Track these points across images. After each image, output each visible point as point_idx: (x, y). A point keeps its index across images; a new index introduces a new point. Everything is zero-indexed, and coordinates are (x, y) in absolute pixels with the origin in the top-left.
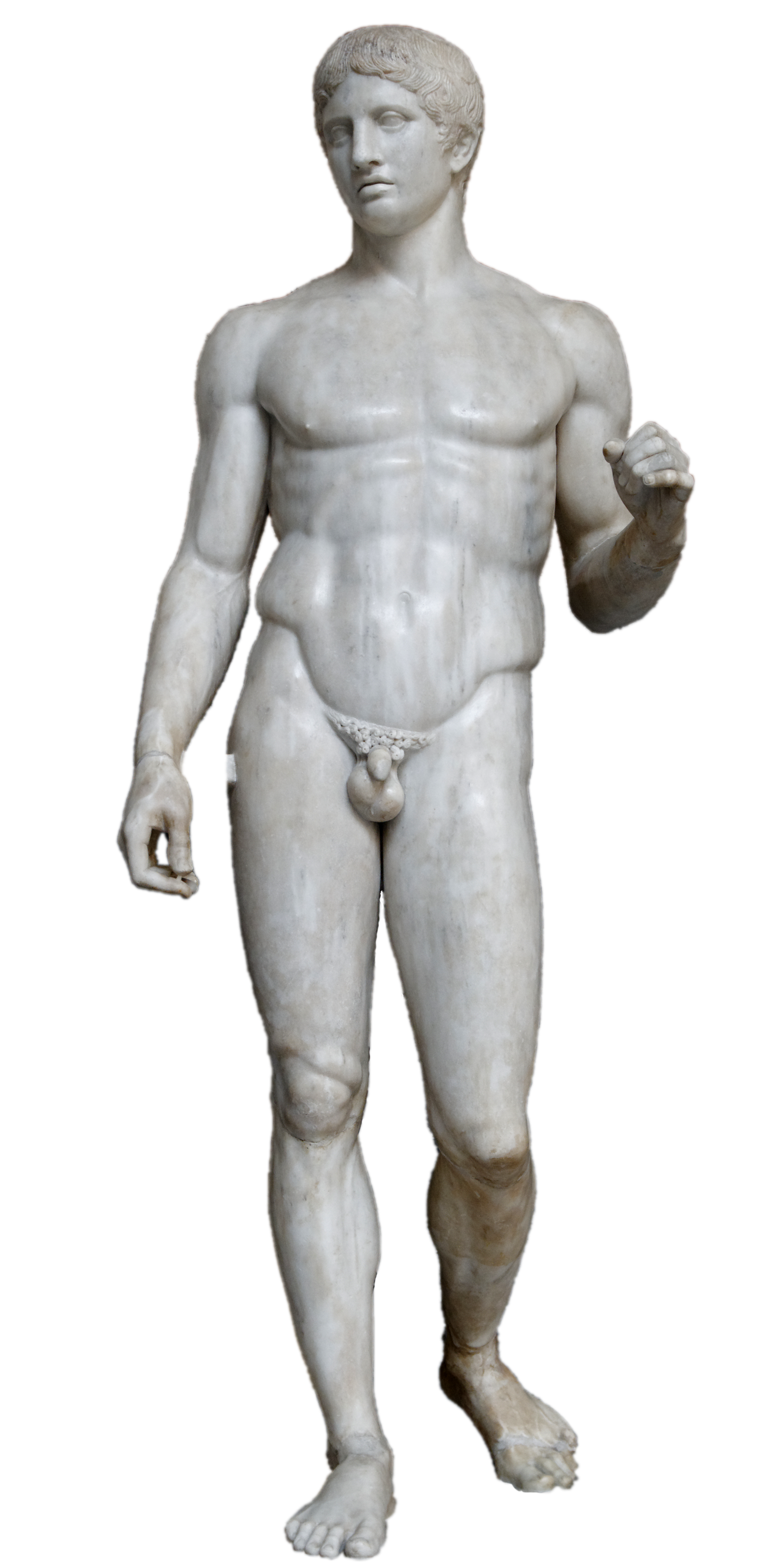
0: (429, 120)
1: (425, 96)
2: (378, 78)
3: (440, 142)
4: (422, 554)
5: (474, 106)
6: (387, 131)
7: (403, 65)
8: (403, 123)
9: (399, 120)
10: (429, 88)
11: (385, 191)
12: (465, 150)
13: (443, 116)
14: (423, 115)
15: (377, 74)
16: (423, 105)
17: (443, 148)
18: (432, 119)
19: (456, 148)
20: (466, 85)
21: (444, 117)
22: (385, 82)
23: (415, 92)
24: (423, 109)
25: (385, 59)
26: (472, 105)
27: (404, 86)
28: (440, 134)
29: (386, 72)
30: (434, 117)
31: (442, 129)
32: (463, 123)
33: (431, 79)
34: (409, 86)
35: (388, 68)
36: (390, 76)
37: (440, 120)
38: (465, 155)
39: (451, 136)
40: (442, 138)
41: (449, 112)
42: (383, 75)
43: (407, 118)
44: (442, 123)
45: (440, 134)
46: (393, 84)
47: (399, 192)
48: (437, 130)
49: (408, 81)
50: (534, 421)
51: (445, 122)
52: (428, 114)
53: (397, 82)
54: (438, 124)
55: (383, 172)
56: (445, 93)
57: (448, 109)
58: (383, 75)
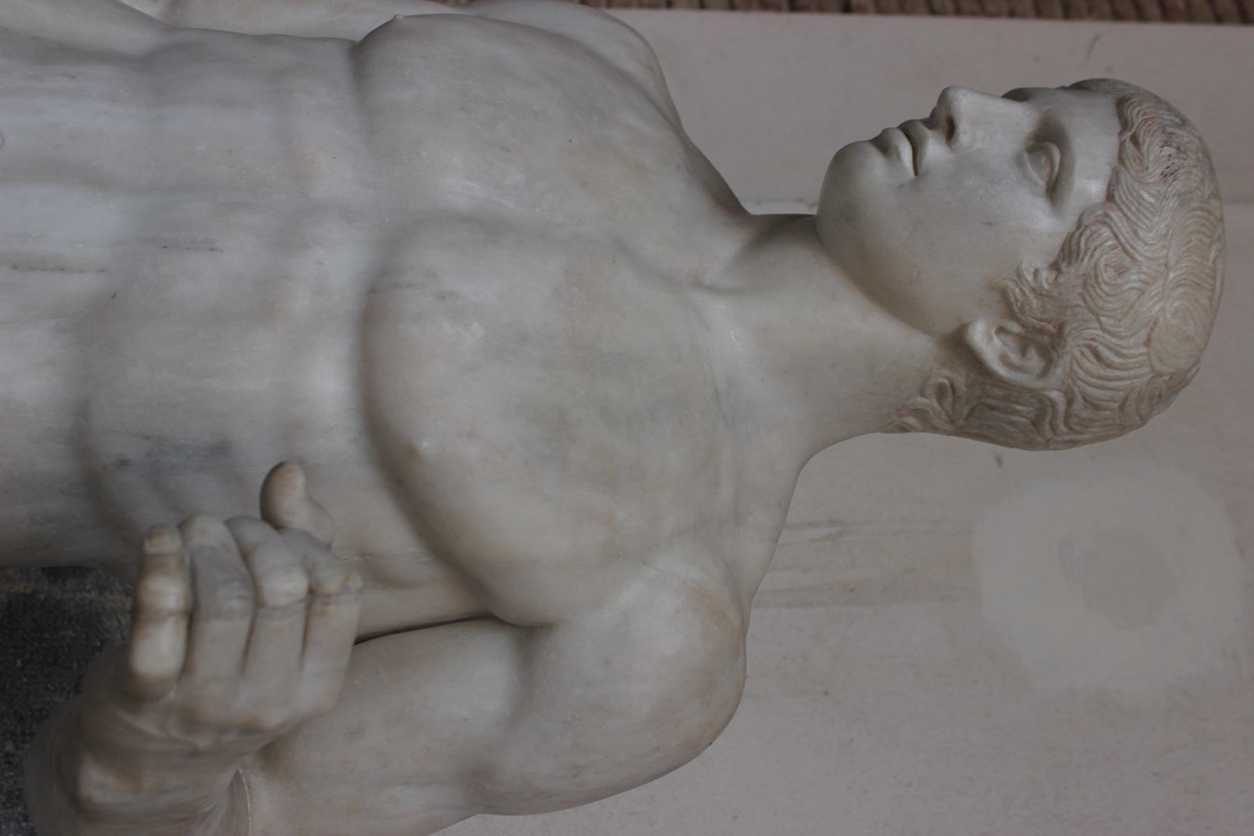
0: (1059, 242)
1: (1105, 221)
2: (1118, 128)
3: (1019, 275)
4: (93, 180)
5: (1109, 366)
6: (1019, 161)
7: (1155, 172)
8: (1042, 184)
9: (1046, 171)
10: (1123, 228)
11: (899, 156)
12: (1014, 358)
13: (1072, 270)
14: (1067, 225)
15: (1125, 125)
16: (1085, 222)
17: (1011, 285)
18: (1063, 249)
19: (1015, 328)
20: (1143, 334)
21: (1072, 273)
22: (1113, 141)
23: (1110, 197)
24: (1079, 224)
25: (1159, 138)
26: (1106, 353)
27: (1115, 174)
28: (1036, 273)
29: (1135, 140)
30: (1069, 252)
31: (1045, 275)
32: (1067, 330)
33: (1141, 234)
34: (1118, 182)
35: (1146, 141)
36: (1129, 146)
37: (1063, 266)
38: (1004, 359)
39: (1035, 303)
40: (1030, 278)
41: (1085, 284)
42: (1128, 135)
43: (1054, 190)
44: (1059, 271)
45: (1036, 273)
46: (1116, 154)
47: (901, 186)
48: (1041, 263)
49: (1126, 178)
50: (426, 445)
51: (1062, 279)
52: (1071, 236)
53: (1121, 159)
54: (1055, 266)
55: (934, 149)
56: (1121, 271)
57: (1090, 281)
58: (1128, 135)
